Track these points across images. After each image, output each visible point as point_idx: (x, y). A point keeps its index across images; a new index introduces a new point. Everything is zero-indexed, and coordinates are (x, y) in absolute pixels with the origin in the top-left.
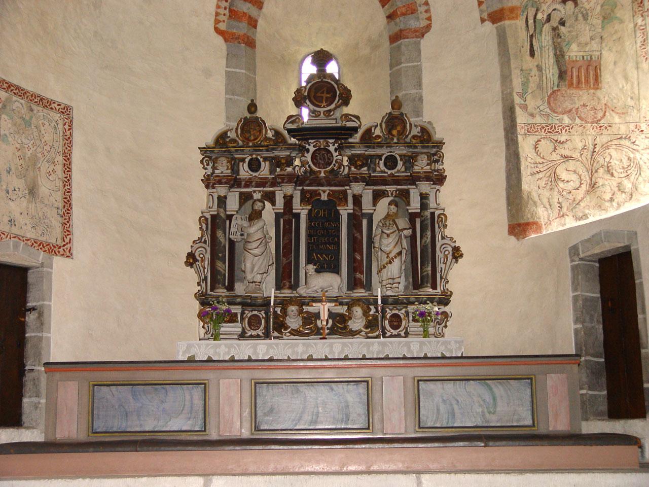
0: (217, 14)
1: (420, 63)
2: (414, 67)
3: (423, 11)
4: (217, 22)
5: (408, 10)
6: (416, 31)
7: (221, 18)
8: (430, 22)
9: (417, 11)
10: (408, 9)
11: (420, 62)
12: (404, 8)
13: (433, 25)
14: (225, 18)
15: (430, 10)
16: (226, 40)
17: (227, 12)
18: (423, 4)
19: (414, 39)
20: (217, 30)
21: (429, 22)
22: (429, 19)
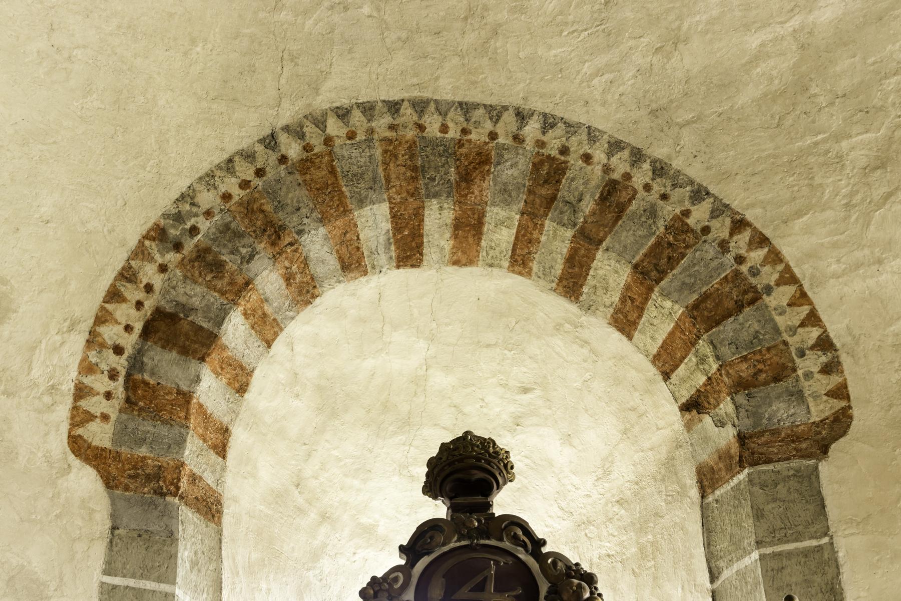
0: (81, 392)
1: (826, 540)
2: (806, 553)
3: (815, 369)
4: (79, 417)
5: (761, 371)
6: (795, 438)
7: (95, 405)
8: (844, 404)
9: (794, 370)
10: (760, 366)
11: (826, 534)
12: (744, 366)
13: (856, 412)
14: (112, 408)
15: (839, 363)
16: (109, 483)
17: (118, 387)
18: (812, 348)
19: (796, 463)
20: (77, 445)
21: (840, 404)
22: (840, 392)
